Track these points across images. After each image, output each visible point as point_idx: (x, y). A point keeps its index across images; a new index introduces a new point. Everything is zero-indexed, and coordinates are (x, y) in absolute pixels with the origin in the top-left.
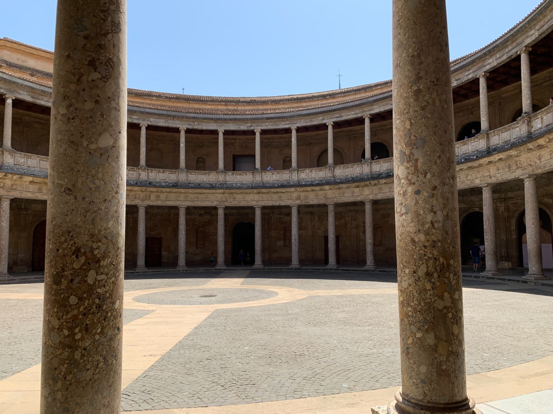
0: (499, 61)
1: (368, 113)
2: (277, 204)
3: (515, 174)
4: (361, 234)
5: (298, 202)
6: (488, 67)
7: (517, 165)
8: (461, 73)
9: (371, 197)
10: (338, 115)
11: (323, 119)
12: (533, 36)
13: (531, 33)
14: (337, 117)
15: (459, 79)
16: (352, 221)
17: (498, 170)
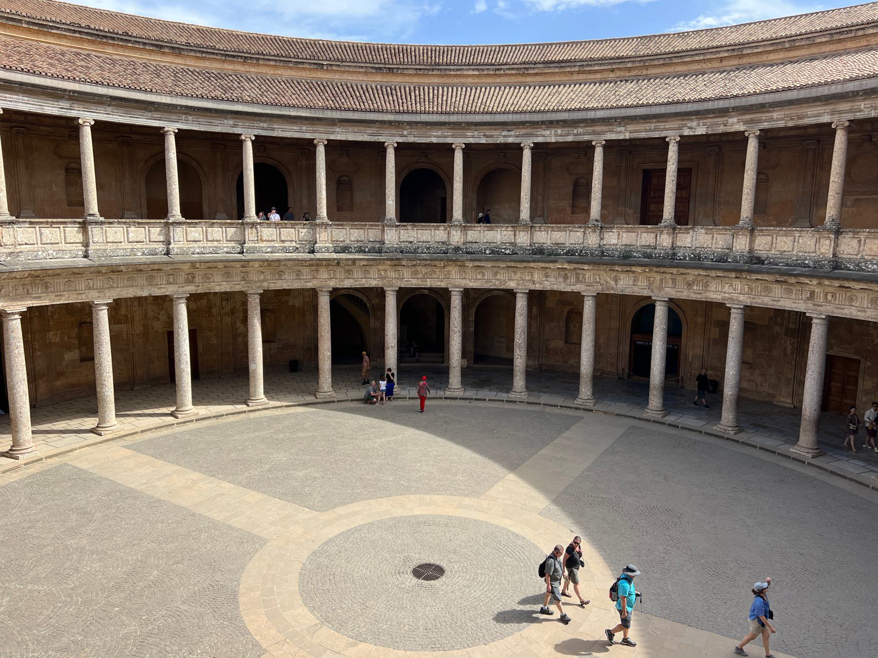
0: (561, 139)
1: (325, 136)
2: (145, 294)
3: (573, 287)
4: (239, 325)
5: (191, 289)
6: (540, 140)
7: (578, 278)
8: (496, 129)
9: (333, 284)
10: (265, 125)
11: (235, 126)
12: (623, 133)
13: (619, 129)
14: (263, 129)
15: (491, 136)
16: (224, 303)
17: (547, 277)
